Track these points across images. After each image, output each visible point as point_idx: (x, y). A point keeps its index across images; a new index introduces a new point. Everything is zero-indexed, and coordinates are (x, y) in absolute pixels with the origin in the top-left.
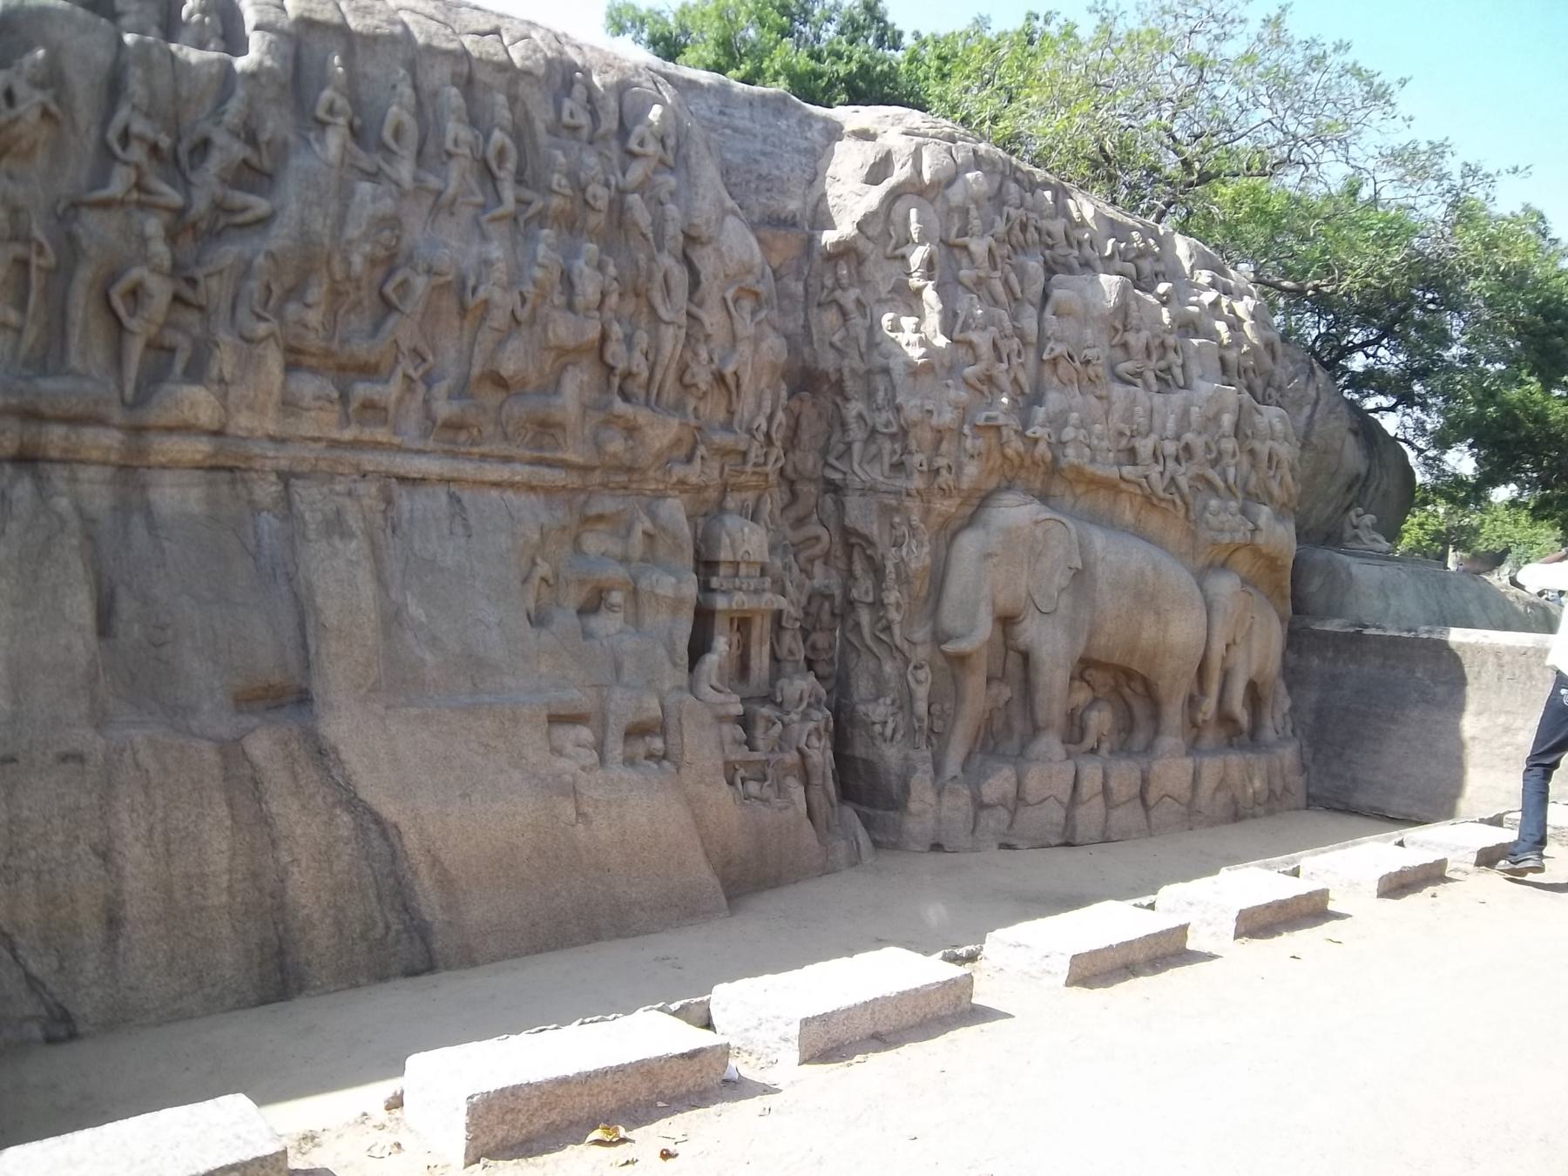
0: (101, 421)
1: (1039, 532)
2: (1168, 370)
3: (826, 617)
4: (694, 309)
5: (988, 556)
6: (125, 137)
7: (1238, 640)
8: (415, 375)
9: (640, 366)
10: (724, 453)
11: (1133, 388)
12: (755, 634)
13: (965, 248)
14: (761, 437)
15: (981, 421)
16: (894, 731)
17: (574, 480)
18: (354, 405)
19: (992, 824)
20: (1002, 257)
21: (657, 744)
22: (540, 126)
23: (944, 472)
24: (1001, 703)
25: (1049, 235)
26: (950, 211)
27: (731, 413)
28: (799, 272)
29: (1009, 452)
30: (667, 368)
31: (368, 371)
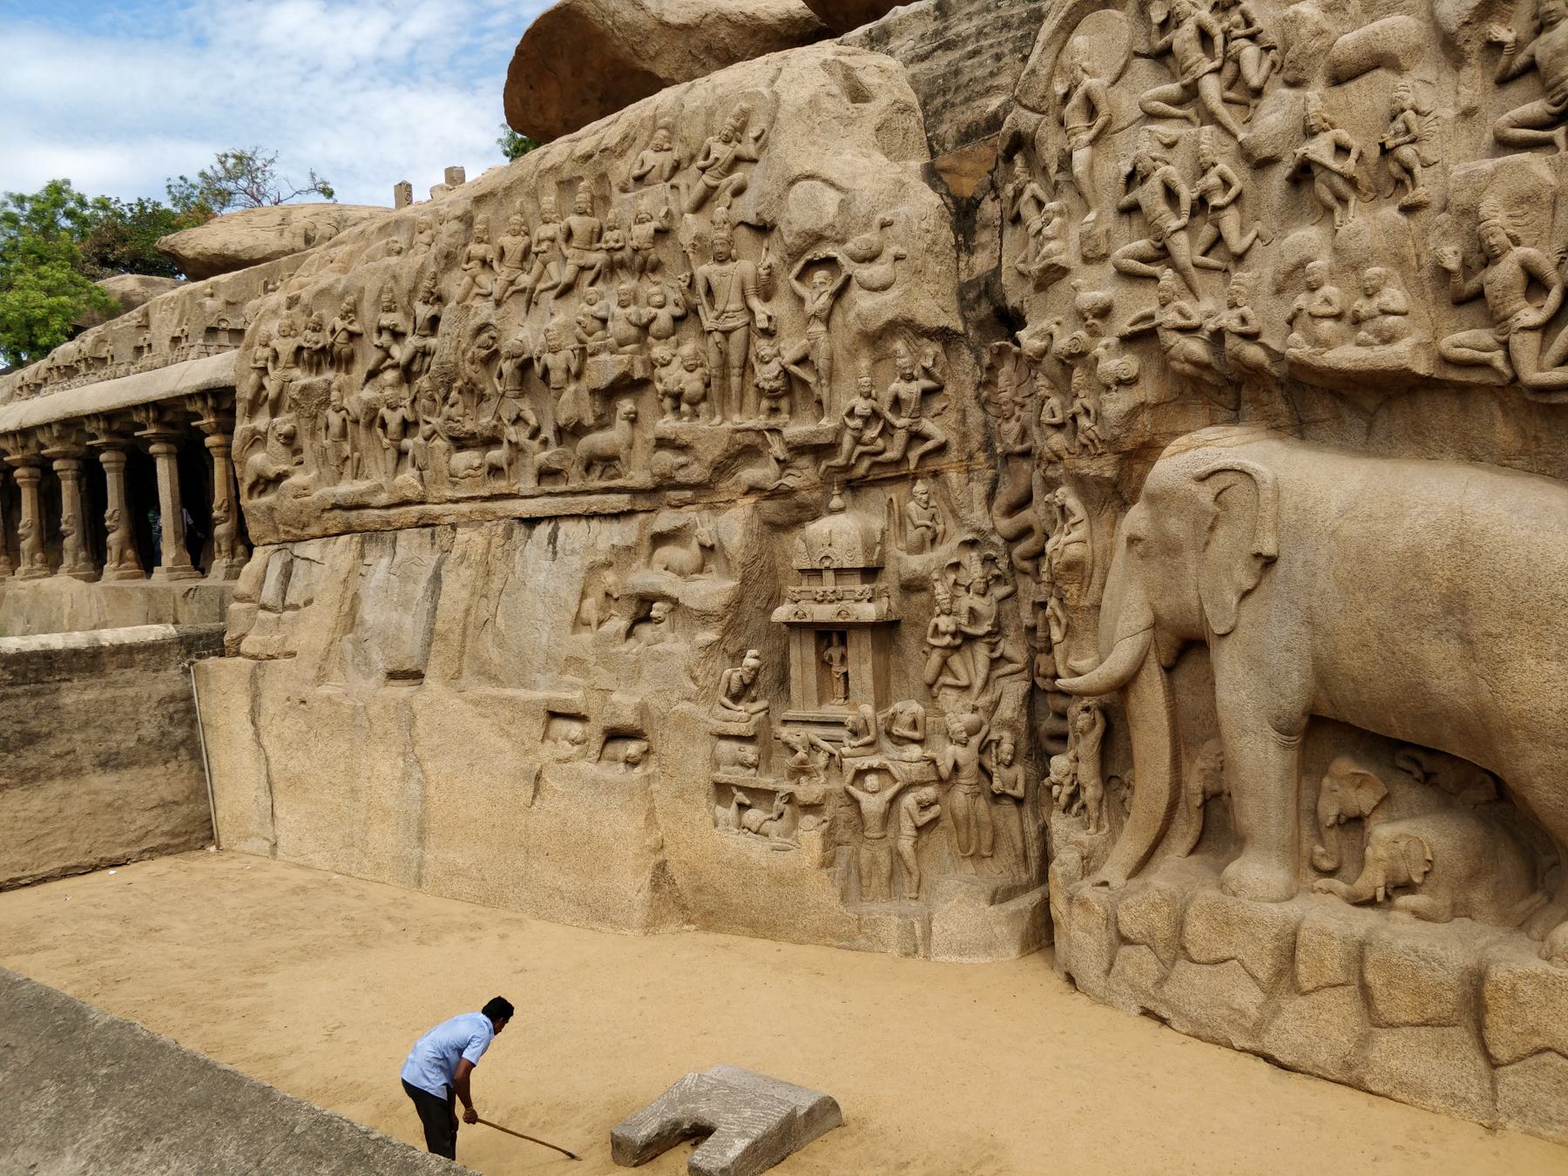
0: (366, 506)
1: (1205, 494)
4: (755, 303)
5: (1133, 541)
6: (380, 330)
8: (514, 438)
9: (692, 384)
10: (818, 450)
11: (1488, 165)
12: (851, 653)
14: (858, 423)
15: (1123, 325)
16: (1074, 796)
17: (642, 504)
18: (485, 470)
19: (1130, 972)
20: (1226, 33)
21: (633, 748)
22: (615, 190)
23: (1084, 422)
27: (820, 402)
29: (1177, 366)
30: (725, 377)
31: (492, 441)
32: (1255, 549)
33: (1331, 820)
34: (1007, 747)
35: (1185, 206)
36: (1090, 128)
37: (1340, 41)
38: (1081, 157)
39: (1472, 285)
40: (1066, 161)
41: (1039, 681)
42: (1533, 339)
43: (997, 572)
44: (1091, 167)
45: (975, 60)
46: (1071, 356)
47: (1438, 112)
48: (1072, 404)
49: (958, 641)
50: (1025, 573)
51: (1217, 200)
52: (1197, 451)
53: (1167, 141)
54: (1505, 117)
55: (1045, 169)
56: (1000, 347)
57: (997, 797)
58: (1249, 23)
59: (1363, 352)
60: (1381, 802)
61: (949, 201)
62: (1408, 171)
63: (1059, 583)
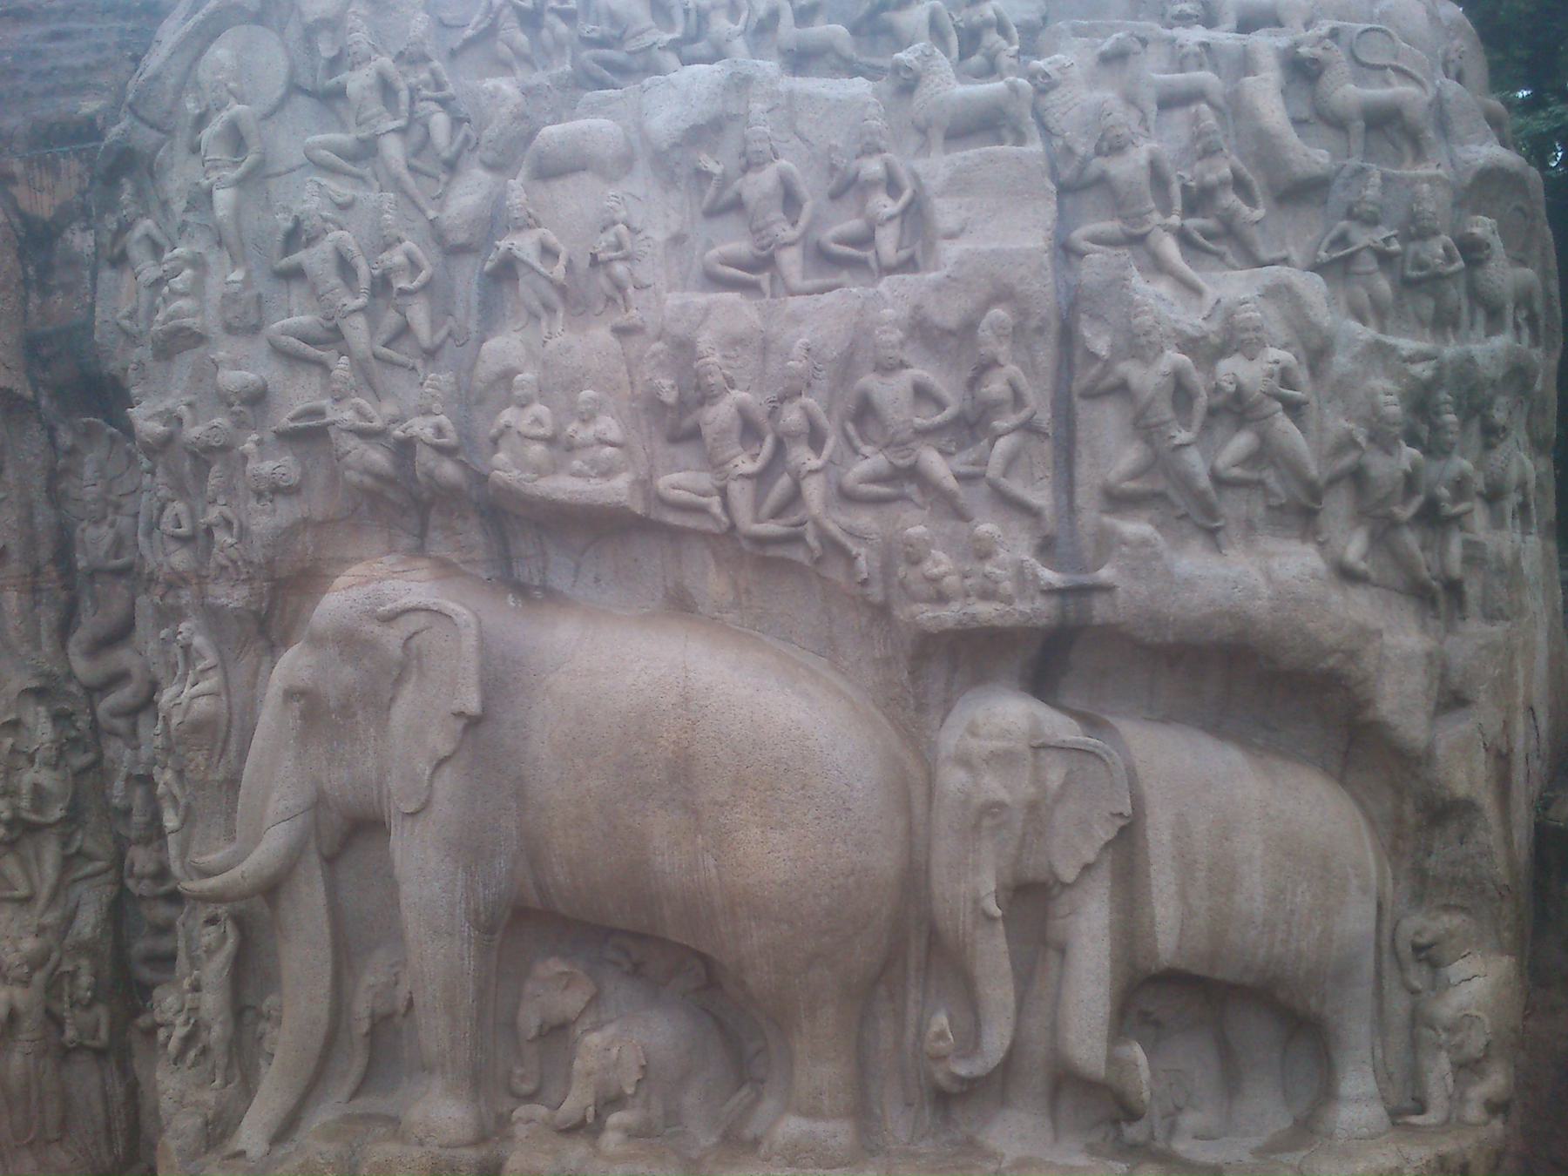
1: (392, 638)
2: (865, 240)
3: (138, 818)
5: (290, 694)
7: (1068, 873)
11: (701, 299)
13: (340, 93)
15: (284, 422)
16: (188, 1040)
20: (413, 91)
23: (223, 538)
24: (401, 1006)
25: (613, 18)
26: (309, 34)
28: (85, 211)
29: (353, 476)
32: (456, 706)
33: (533, 1032)
34: (85, 980)
35: (364, 284)
36: (236, 164)
37: (547, 131)
38: (224, 198)
39: (688, 422)
40: (202, 199)
41: (130, 883)
42: (748, 486)
43: (73, 733)
44: (238, 211)
45: (63, 45)
46: (210, 449)
47: (649, 232)
48: (204, 511)
49: (15, 834)
50: (114, 733)
51: (402, 283)
52: (373, 585)
53: (340, 200)
54: (714, 253)
55: (165, 205)
56: (88, 424)
57: (66, 1053)
58: (439, 86)
59: (578, 485)
60: (589, 1003)
61: (16, 221)
62: (619, 287)
63: (180, 750)
